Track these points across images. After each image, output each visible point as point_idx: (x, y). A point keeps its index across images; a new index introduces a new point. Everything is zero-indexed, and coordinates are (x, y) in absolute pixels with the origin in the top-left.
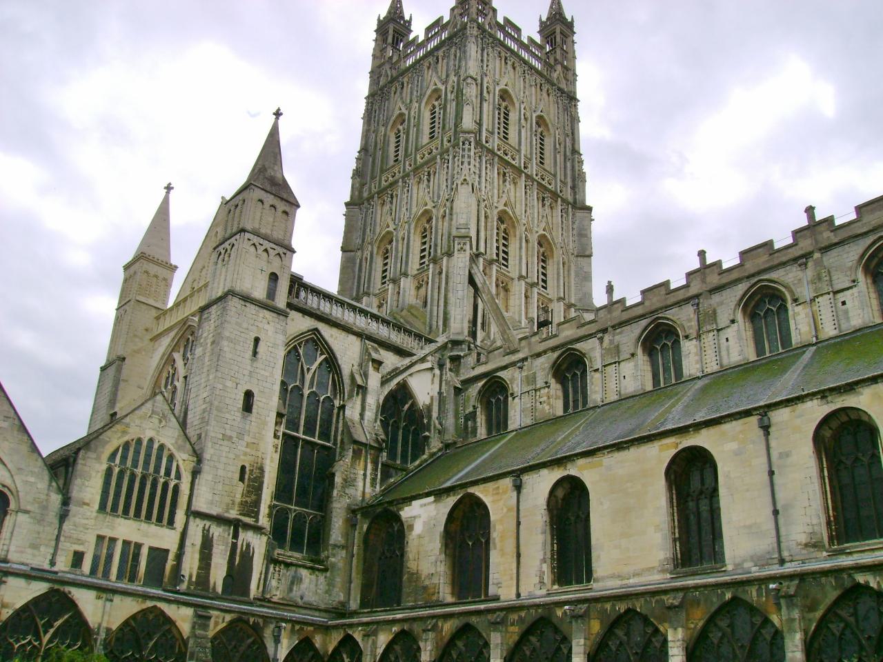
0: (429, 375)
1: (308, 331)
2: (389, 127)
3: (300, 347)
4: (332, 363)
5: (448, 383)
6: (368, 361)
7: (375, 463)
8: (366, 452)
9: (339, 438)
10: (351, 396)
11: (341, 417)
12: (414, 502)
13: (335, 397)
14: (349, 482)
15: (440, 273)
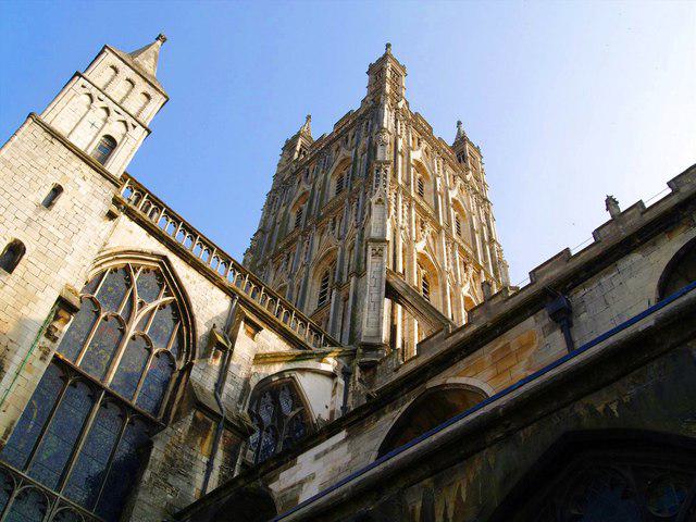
0: (327, 383)
1: (153, 255)
2: (290, 207)
3: (135, 272)
4: (182, 309)
5: (356, 394)
6: (239, 323)
7: (231, 453)
8: (217, 430)
9: (174, 409)
10: (205, 356)
11: (183, 381)
12: (300, 459)
13: (179, 358)
14: (177, 467)
15: (346, 299)
